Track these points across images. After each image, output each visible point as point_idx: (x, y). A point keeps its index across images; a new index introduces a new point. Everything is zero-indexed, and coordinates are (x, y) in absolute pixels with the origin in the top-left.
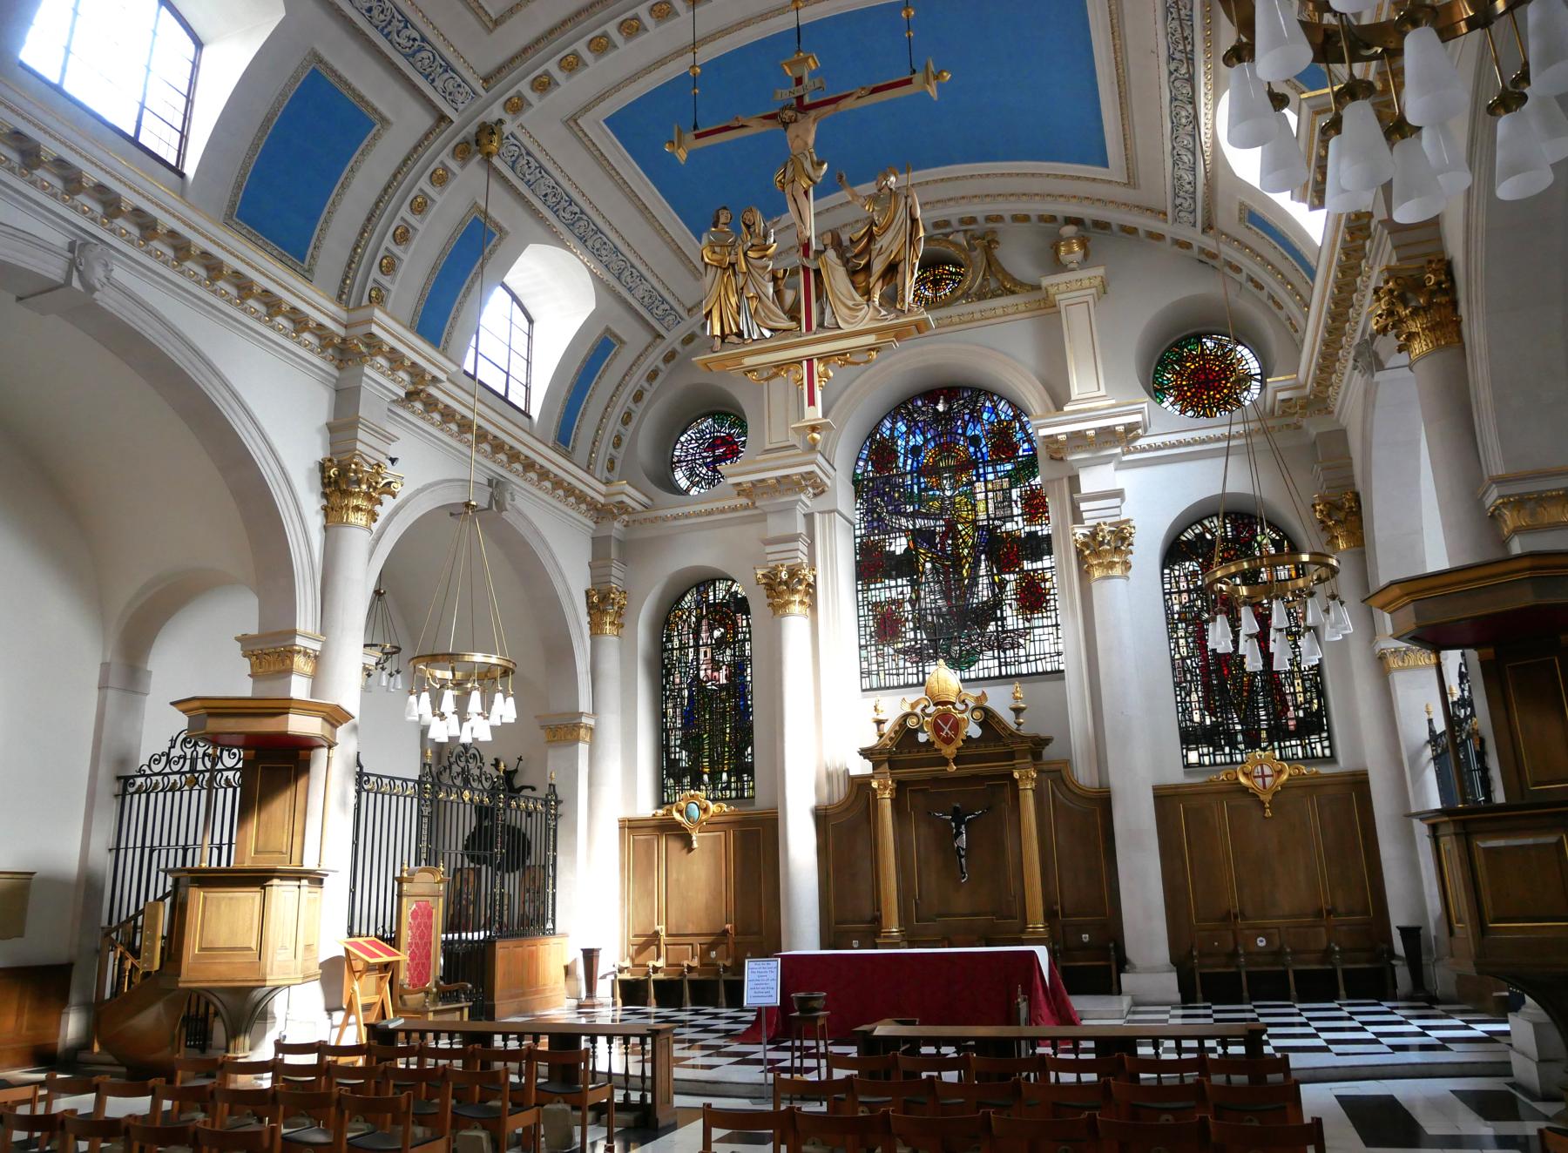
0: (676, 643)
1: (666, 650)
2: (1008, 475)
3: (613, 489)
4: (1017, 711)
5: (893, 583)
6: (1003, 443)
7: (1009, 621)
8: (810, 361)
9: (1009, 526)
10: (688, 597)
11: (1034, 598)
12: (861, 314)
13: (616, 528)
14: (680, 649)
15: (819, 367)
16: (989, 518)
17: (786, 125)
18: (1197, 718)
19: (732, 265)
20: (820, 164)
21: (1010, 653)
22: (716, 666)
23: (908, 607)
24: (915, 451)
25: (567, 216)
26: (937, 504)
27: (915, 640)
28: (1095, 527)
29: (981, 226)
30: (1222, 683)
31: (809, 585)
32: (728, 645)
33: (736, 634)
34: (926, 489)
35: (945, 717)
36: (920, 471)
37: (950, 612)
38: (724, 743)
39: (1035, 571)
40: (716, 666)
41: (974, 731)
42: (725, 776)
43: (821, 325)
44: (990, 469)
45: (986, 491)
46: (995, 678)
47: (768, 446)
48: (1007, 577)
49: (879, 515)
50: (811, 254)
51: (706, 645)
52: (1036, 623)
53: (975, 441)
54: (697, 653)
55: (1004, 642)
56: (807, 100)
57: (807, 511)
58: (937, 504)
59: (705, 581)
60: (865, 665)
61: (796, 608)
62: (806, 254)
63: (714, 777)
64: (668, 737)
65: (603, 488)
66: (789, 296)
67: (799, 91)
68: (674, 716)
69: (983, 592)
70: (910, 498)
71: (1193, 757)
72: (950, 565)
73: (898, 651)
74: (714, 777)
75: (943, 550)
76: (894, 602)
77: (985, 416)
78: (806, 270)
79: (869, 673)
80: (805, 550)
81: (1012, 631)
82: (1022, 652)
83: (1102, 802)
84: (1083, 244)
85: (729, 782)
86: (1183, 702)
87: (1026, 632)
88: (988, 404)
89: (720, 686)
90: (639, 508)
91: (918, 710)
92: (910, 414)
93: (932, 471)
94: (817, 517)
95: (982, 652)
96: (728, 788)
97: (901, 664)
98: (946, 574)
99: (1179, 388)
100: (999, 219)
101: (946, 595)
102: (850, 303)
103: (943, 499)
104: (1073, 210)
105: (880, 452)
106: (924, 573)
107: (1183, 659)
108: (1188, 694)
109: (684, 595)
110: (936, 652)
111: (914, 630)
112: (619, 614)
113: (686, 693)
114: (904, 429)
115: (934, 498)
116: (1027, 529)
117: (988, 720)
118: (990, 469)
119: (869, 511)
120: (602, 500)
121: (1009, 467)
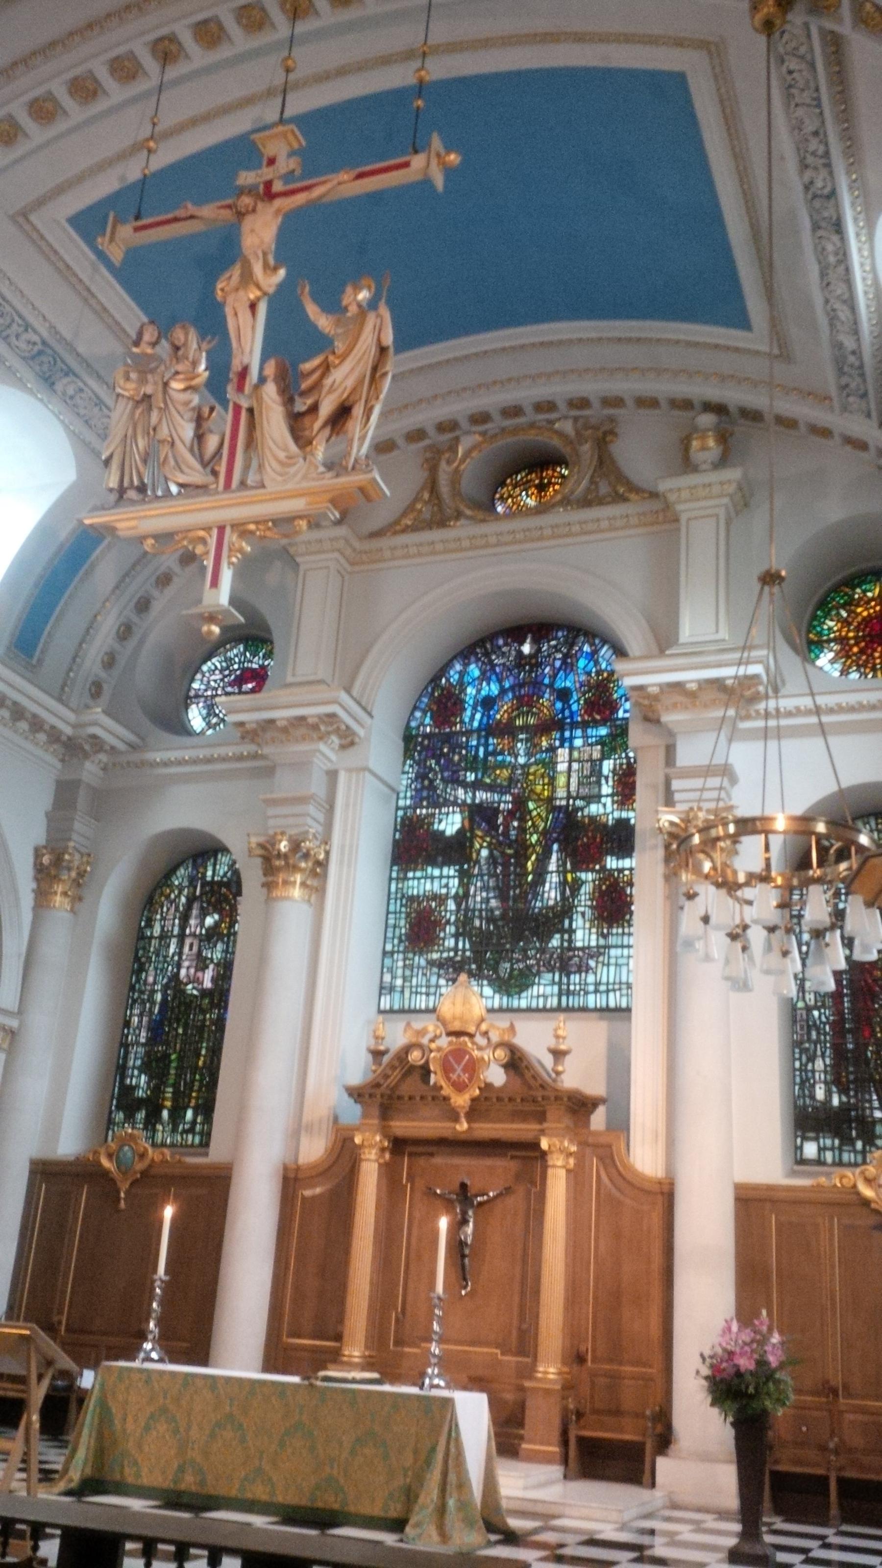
0: (157, 931)
2: (601, 742)
3: (86, 718)
4: (558, 1054)
5: (437, 872)
6: (601, 701)
7: (579, 934)
8: (221, 529)
9: (594, 809)
10: (181, 871)
11: (614, 906)
12: (292, 470)
13: (90, 770)
15: (230, 537)
16: (569, 797)
17: (241, 215)
18: (820, 1093)
19: (147, 397)
20: (275, 269)
21: (575, 978)
22: (202, 963)
23: (451, 905)
24: (488, 703)
25: (23, 345)
26: (506, 773)
27: (456, 949)
28: (687, 813)
29: (595, 413)
30: (860, 1048)
31: (318, 863)
32: (220, 937)
34: (494, 753)
35: (459, 1053)
36: (490, 730)
37: (503, 916)
38: (195, 1069)
39: (621, 871)
40: (202, 963)
41: (496, 1076)
42: (189, 1114)
43: (243, 484)
44: (579, 733)
45: (571, 761)
46: (552, 1010)
47: (290, 679)
48: (583, 876)
49: (431, 782)
50: (247, 389)
51: (193, 935)
52: (612, 940)
53: (564, 695)
54: (181, 944)
55: (568, 963)
56: (278, 187)
57: (329, 766)
58: (506, 773)
59: (206, 850)
60: (387, 978)
61: (296, 892)
62: (240, 388)
63: (177, 1114)
64: (127, 1053)
65: (71, 717)
66: (212, 442)
67: (267, 173)
68: (139, 1027)
69: (550, 893)
70: (473, 764)
71: (810, 1150)
72: (512, 855)
73: (431, 963)
74: (177, 1114)
75: (506, 833)
76: (435, 897)
77: (582, 663)
78: (237, 409)
79: (392, 989)
80: (321, 817)
81: (582, 949)
82: (591, 978)
83: (665, 1195)
84: (723, 438)
85: (194, 1122)
86: (803, 1069)
87: (599, 952)
88: (587, 648)
89: (204, 993)
90: (121, 746)
91: (425, 1041)
92: (487, 654)
93: (507, 730)
94: (342, 777)
95: (539, 973)
96: (192, 1130)
97: (434, 980)
98: (506, 865)
99: (841, 640)
100: (617, 402)
101: (503, 896)
102: (282, 455)
103: (514, 767)
104: (713, 393)
105: (445, 703)
106: (477, 862)
107: (809, 1009)
108: (812, 1059)
109: (173, 870)
110: (479, 968)
111: (456, 936)
112: (77, 883)
113: (159, 997)
114: (477, 673)
115: (502, 765)
116: (616, 814)
117: (516, 1062)
118: (579, 733)
119: (421, 777)
120: (68, 731)
121: (603, 731)
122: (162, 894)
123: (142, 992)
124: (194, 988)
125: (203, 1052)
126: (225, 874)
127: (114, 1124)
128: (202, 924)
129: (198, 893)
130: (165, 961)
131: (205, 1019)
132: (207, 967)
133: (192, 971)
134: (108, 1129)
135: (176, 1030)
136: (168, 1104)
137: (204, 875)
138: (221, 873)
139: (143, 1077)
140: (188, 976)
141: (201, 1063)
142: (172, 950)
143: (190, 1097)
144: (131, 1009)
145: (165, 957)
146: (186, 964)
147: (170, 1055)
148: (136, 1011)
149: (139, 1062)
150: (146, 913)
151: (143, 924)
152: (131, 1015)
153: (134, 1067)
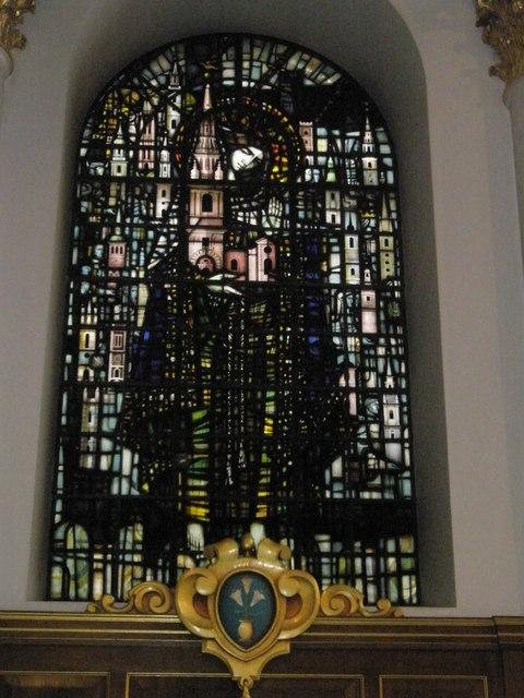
0: (119, 163)
14: (130, 181)
22: (238, 237)
32: (274, 191)
38: (256, 442)
40: (238, 237)
51: (209, 182)
64: (76, 407)
89: (251, 290)
109: (147, 59)
113: (143, 294)
122: (121, 100)
123: (103, 282)
124: (223, 282)
125: (270, 408)
126: (264, 79)
127: (64, 552)
128: (227, 167)
129: (207, 105)
130: (147, 227)
131: (262, 344)
133: (217, 249)
134: (51, 564)
135: (197, 360)
137: (217, 77)
138: (256, 75)
139: (127, 454)
140: (207, 257)
141: (268, 430)
142: (161, 206)
143: (255, 501)
145: (148, 218)
149: (110, 424)
150: (87, 133)
151: (83, 152)
152: (78, 327)
153: (99, 434)
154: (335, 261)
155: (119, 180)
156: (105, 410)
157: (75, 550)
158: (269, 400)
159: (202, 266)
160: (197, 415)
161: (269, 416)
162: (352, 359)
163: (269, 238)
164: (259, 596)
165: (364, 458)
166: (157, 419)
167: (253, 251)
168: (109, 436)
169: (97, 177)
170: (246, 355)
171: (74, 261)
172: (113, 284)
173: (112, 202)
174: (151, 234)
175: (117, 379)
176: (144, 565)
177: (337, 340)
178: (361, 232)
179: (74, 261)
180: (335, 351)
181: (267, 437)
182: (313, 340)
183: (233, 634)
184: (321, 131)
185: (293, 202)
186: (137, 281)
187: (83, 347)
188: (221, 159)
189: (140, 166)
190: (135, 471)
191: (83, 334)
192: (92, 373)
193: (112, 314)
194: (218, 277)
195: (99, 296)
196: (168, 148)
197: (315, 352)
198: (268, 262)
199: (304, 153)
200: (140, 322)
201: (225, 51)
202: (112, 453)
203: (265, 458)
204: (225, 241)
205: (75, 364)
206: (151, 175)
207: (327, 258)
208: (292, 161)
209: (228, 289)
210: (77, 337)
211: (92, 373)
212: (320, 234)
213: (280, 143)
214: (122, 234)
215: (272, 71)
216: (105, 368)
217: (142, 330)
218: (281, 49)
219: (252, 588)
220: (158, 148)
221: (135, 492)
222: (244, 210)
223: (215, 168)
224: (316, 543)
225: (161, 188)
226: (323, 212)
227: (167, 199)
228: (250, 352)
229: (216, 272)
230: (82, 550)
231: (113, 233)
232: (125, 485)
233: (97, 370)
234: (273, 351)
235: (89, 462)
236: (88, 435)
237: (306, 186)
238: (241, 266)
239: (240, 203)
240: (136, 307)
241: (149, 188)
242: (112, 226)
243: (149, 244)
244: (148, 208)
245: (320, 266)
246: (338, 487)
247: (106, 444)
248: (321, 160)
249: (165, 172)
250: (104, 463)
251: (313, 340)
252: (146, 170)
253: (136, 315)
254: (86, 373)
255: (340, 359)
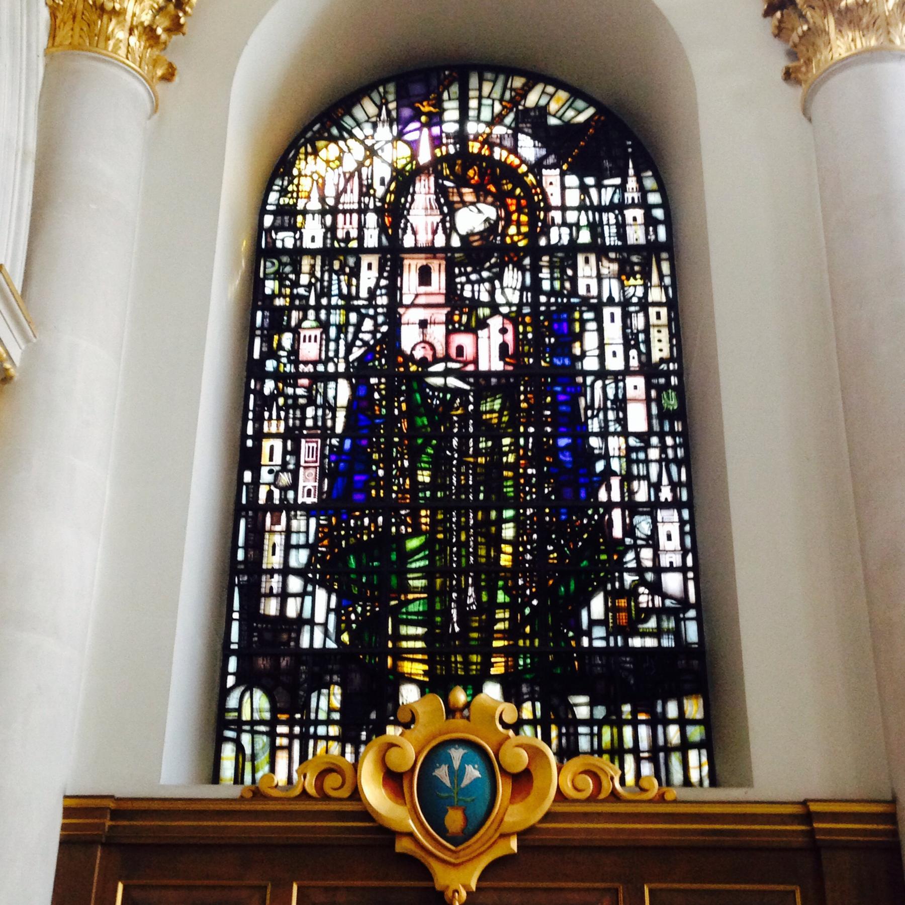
1: (272, 252)
14: (327, 254)
22: (463, 313)
32: (510, 256)
33: (539, 227)
38: (490, 573)
51: (430, 250)
89: (483, 384)
113: (342, 392)
123: (291, 379)
124: (446, 373)
125: (508, 532)
127: (238, 725)
130: (348, 308)
131: (497, 448)
132: (483, 324)
133: (437, 334)
134: (220, 740)
135: (412, 473)
136: (415, 668)
138: (486, 115)
141: (505, 560)
142: (368, 278)
143: (488, 654)
144: (259, 420)
146: (411, 316)
147: (401, 539)
148: (273, 426)
149: (299, 558)
150: (273, 197)
151: (268, 220)
152: (259, 436)
153: (286, 571)
154: (591, 340)
155: (313, 253)
156: (294, 540)
157: (253, 723)
158: (507, 521)
159: (418, 354)
160: (413, 544)
161: (507, 542)
162: (615, 465)
163: (505, 316)
164: (473, 773)
165: (633, 593)
166: (358, 549)
167: (482, 333)
168: (298, 572)
169: (284, 251)
170: (476, 464)
171: (256, 355)
172: (304, 382)
173: (304, 279)
174: (353, 317)
175: (309, 501)
176: (342, 740)
177: (595, 442)
178: (625, 304)
179: (256, 355)
180: (591, 457)
181: (504, 569)
182: (563, 442)
183: (441, 828)
184: (572, 180)
185: (535, 269)
186: (335, 377)
187: (265, 459)
188: (443, 221)
189: (340, 234)
190: (332, 617)
191: (266, 444)
192: (277, 493)
193: (303, 418)
194: (439, 367)
195: (286, 397)
196: (378, 211)
197: (566, 458)
198: (503, 347)
199: (548, 208)
200: (339, 429)
201: (447, 88)
202: (302, 595)
203: (501, 597)
204: (449, 320)
205: (256, 482)
206: (354, 244)
207: (580, 337)
208: (532, 223)
209: (453, 382)
210: (258, 448)
211: (277, 493)
212: (571, 308)
213: (518, 198)
214: (318, 319)
215: (507, 110)
216: (294, 486)
217: (342, 437)
218: (518, 82)
219: (464, 761)
220: (362, 211)
221: (331, 645)
222: (473, 283)
223: (435, 232)
224: (571, 707)
225: (365, 260)
226: (574, 280)
227: (375, 273)
228: (482, 460)
229: (436, 360)
230: (262, 722)
231: (305, 318)
232: (318, 633)
233: (284, 490)
234: (511, 458)
235: (271, 607)
236: (271, 572)
237: (551, 249)
238: (469, 353)
239: (467, 275)
240: (334, 410)
241: (351, 261)
242: (305, 309)
243: (351, 329)
244: (349, 285)
245: (570, 348)
246: (599, 632)
247: (295, 584)
248: (572, 217)
249: (371, 241)
250: (292, 611)
251: (563, 442)
252: (348, 239)
253: (334, 418)
254: (270, 494)
255: (600, 466)
